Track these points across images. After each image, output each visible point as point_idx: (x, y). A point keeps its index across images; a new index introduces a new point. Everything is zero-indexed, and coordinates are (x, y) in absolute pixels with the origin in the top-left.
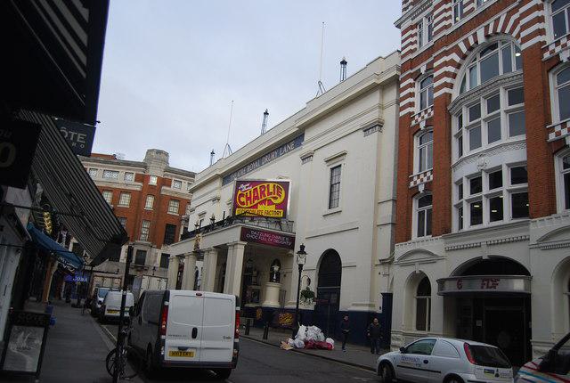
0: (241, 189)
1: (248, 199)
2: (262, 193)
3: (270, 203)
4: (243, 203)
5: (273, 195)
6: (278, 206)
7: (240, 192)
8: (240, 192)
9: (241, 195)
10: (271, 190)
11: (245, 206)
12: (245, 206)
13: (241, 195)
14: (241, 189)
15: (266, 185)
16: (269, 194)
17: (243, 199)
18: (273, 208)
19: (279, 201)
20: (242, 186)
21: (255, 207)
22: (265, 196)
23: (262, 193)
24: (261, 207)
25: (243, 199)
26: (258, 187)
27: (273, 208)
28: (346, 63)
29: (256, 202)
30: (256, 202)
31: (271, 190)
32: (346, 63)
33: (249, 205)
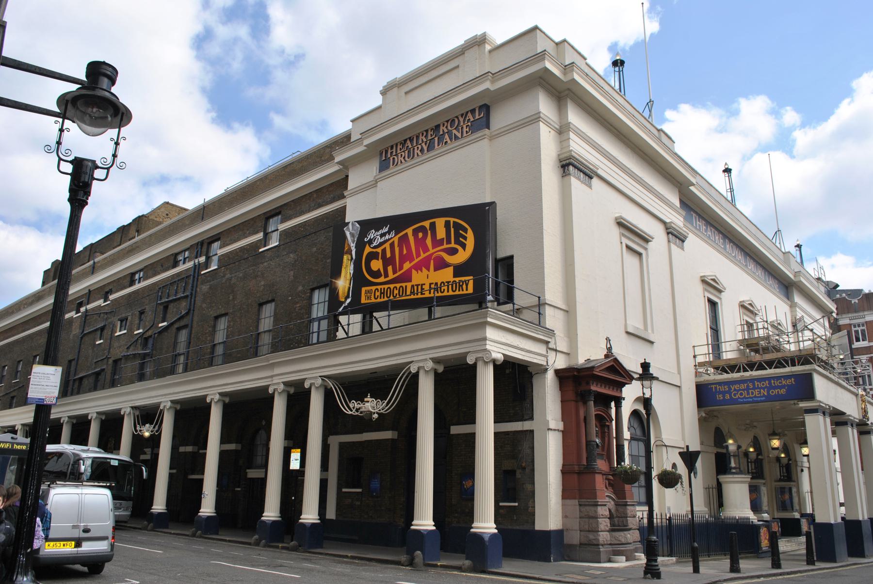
0: (370, 242)
1: (387, 262)
2: (421, 244)
3: (441, 265)
4: (377, 274)
5: (445, 246)
6: (459, 271)
7: (368, 250)
8: (368, 250)
9: (373, 256)
10: (441, 233)
11: (382, 279)
12: (382, 279)
13: (373, 256)
14: (370, 242)
15: (427, 224)
16: (437, 243)
17: (377, 265)
18: (447, 274)
19: (462, 256)
20: (372, 234)
21: (406, 277)
22: (426, 250)
23: (421, 244)
24: (418, 278)
25: (377, 265)
26: (409, 231)
27: (447, 274)
28: (622, 63)
29: (407, 266)
30: (407, 266)
31: (441, 233)
32: (622, 63)
33: (391, 276)
